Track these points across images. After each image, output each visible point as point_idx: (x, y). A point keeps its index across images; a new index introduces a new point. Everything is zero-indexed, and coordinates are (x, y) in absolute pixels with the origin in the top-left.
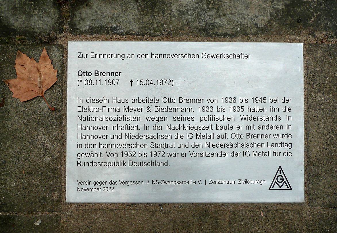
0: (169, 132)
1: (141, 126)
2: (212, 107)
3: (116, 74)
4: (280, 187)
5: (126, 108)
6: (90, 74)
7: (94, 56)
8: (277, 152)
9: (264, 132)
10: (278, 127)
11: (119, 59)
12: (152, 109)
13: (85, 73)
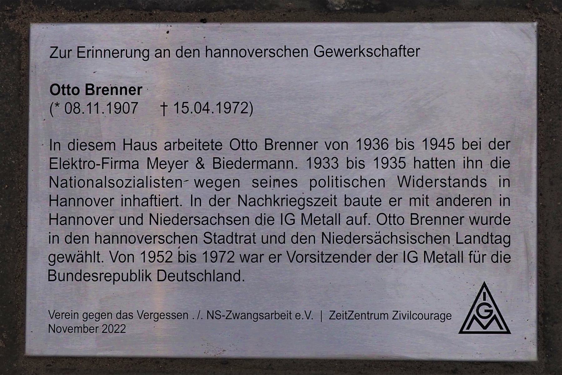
0: (242, 211)
1: (184, 200)
2: (335, 160)
3: (130, 91)
4: (485, 328)
5: (153, 160)
6: (75, 91)
7: (85, 54)
8: (477, 254)
9: (450, 211)
10: (481, 201)
11: (138, 60)
12: (208, 163)
13: (66, 90)
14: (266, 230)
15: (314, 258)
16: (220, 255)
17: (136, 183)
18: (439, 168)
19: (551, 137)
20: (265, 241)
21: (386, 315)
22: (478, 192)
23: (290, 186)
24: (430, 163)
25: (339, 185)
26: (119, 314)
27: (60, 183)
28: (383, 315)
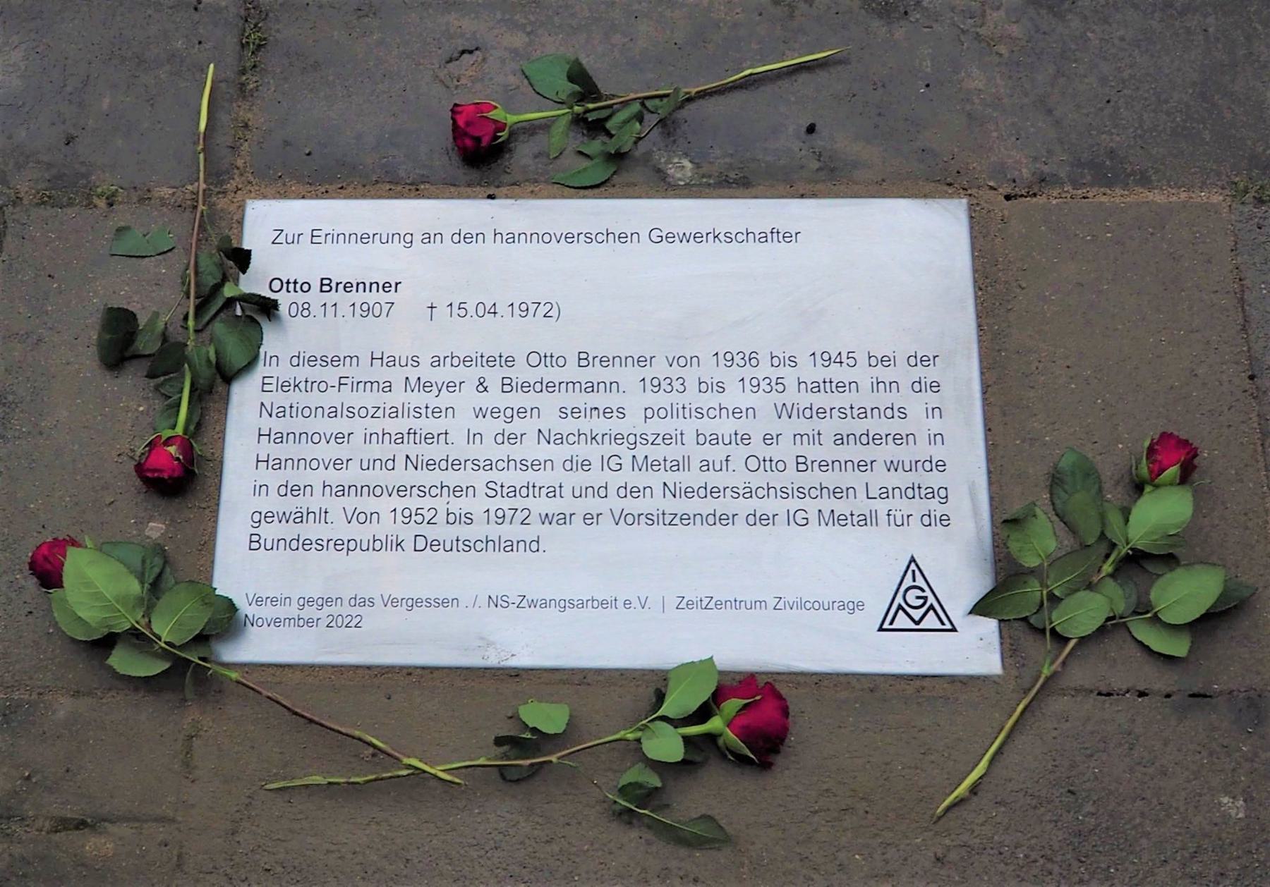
0: (544, 451)
1: (458, 437)
2: (681, 381)
4: (917, 623)
8: (899, 514)
9: (853, 452)
12: (494, 384)
14: (580, 479)
15: (651, 519)
16: (509, 514)
17: (388, 412)
18: (836, 392)
19: (999, 351)
20: (577, 494)
21: (763, 603)
22: (896, 426)
23: (615, 418)
24: (822, 385)
25: (687, 415)
26: (353, 600)
27: (275, 412)
28: (758, 603)
